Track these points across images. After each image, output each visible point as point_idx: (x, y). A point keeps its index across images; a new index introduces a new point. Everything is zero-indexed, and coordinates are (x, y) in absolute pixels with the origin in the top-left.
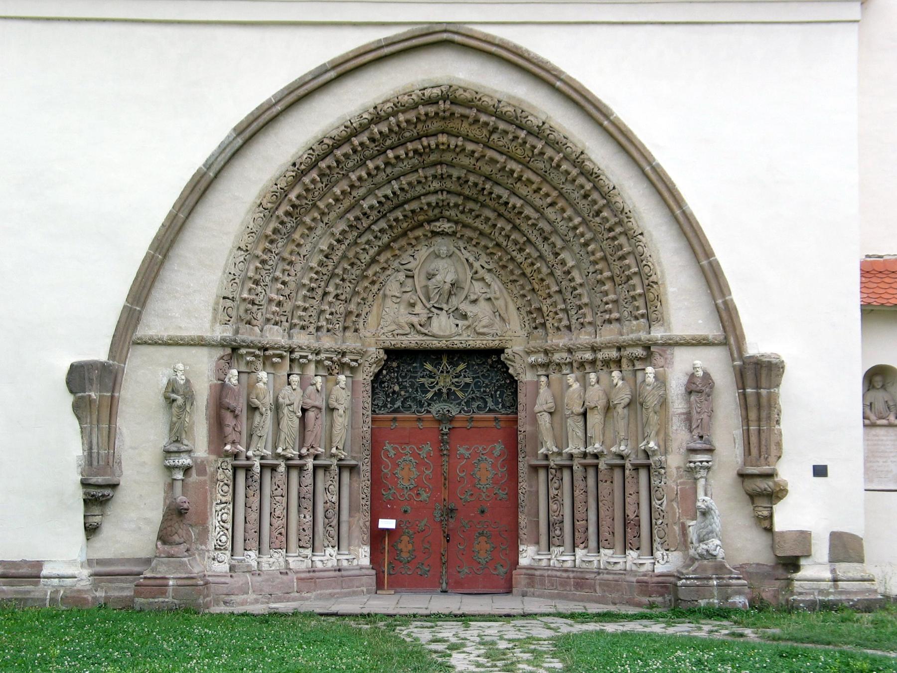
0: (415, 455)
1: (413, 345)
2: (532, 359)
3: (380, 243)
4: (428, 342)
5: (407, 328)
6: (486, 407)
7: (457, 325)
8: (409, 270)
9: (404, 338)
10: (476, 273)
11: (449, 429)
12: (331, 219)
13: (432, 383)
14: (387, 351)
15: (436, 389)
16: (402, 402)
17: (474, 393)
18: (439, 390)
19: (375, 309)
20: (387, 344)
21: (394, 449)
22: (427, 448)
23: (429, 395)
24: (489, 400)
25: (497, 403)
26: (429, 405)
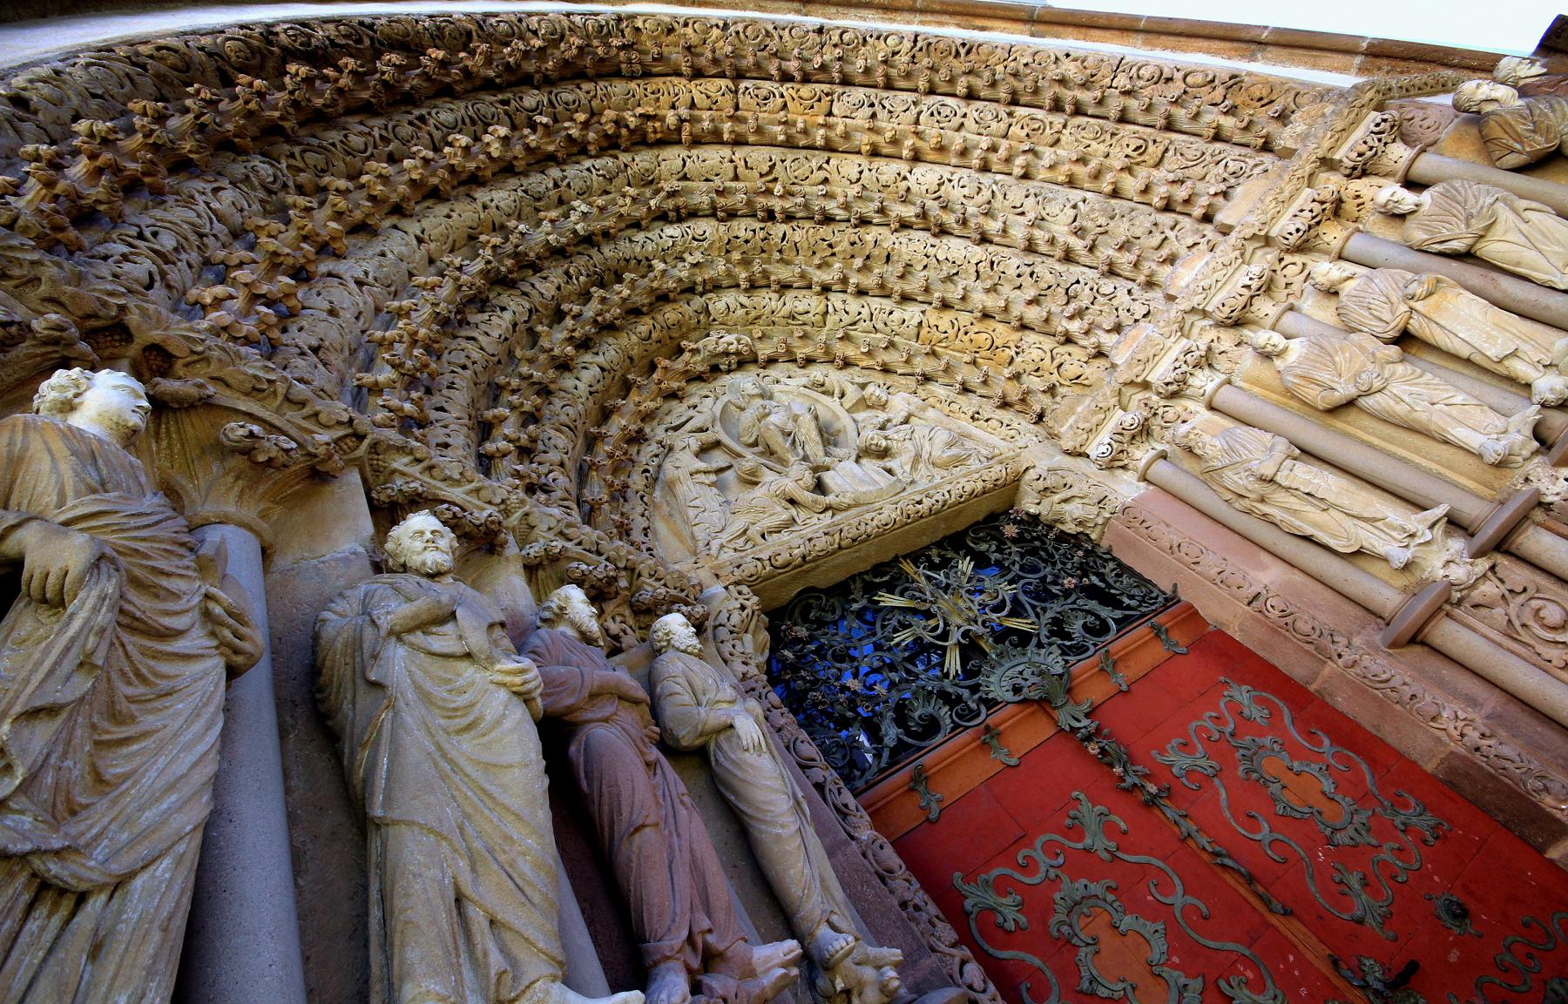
0: (1083, 864)
1: (821, 543)
2: (1099, 446)
3: (600, 359)
4: (855, 522)
5: (779, 509)
6: (1104, 624)
7: (890, 471)
8: (701, 430)
9: (785, 536)
10: (843, 395)
11: (1087, 715)
12: (435, 233)
13: (936, 628)
14: (755, 584)
15: (956, 636)
16: (901, 719)
17: (1044, 610)
18: (965, 634)
19: (661, 527)
20: (750, 567)
21: (1002, 886)
22: (1089, 812)
23: (953, 662)
24: (1093, 605)
25: (1114, 603)
26: (974, 689)
